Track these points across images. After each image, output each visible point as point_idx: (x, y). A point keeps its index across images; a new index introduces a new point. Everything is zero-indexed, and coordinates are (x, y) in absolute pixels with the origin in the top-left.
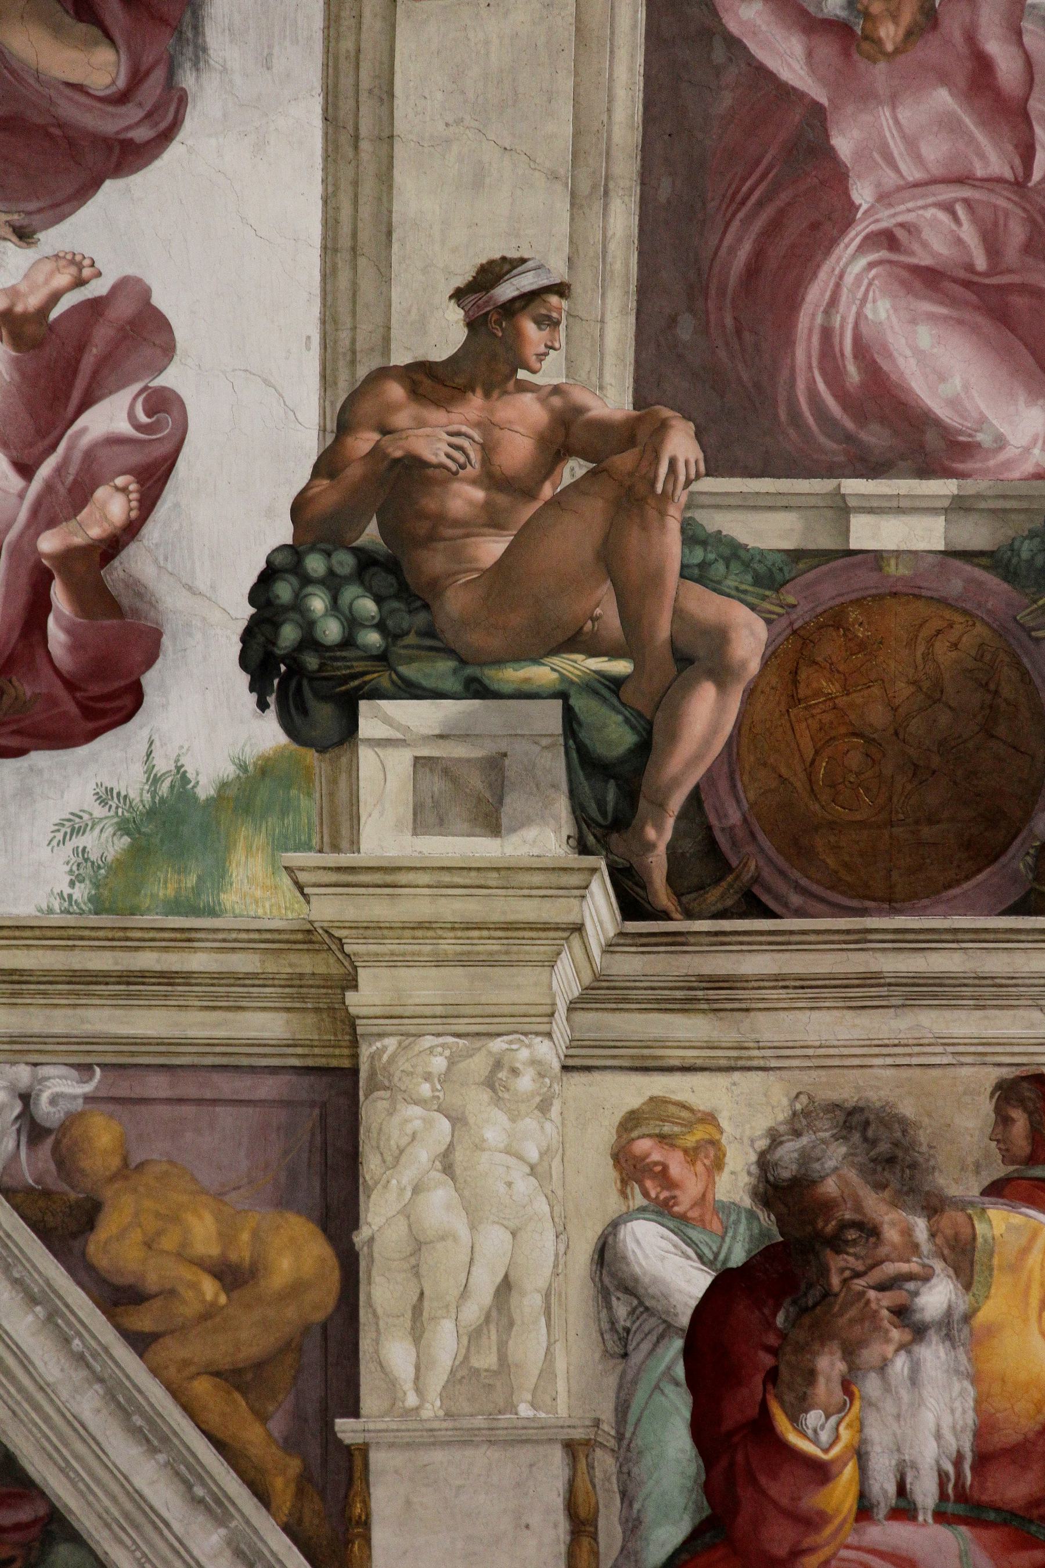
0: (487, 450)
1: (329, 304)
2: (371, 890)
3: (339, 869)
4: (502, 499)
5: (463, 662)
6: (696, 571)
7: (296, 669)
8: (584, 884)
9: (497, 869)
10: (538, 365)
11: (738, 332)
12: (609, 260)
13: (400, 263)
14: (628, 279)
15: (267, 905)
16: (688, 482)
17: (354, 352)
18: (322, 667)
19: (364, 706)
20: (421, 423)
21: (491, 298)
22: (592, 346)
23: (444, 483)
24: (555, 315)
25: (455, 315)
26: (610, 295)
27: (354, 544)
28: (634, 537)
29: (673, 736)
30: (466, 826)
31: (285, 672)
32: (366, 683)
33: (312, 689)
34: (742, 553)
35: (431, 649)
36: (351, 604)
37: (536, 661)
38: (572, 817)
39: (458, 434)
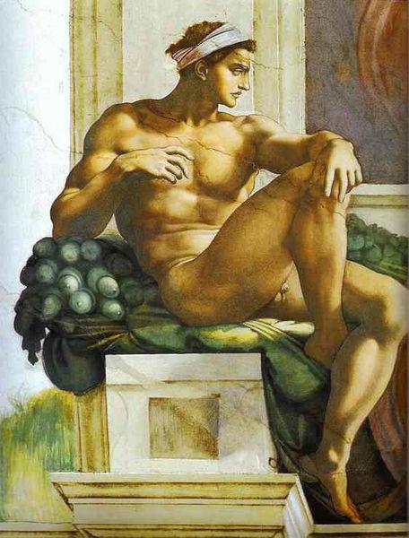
0: (197, 165)
1: (75, 58)
2: (120, 501)
3: (95, 484)
4: (209, 202)
5: (184, 325)
6: (359, 255)
7: (57, 332)
8: (283, 495)
9: (217, 484)
11: (383, 75)
12: (284, 23)
15: (40, 512)
16: (350, 188)
17: (95, 94)
18: (77, 330)
19: (110, 359)
23: (165, 189)
24: (244, 64)
28: (310, 231)
29: (346, 382)
30: (191, 450)
32: (111, 342)
33: (70, 346)
34: (394, 242)
35: (160, 315)
36: (98, 281)
37: (239, 324)
38: (271, 443)
39: (175, 153)
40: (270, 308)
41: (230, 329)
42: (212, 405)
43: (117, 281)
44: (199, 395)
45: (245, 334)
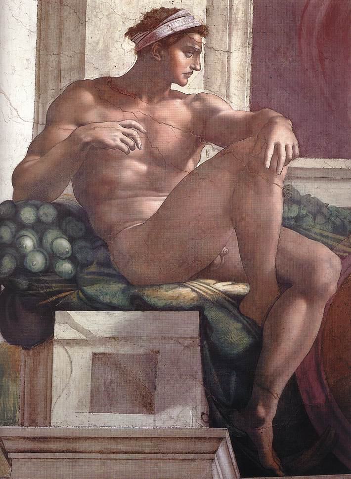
0: (150, 137)
1: (42, 38)
2: (58, 455)
3: (34, 439)
4: (158, 171)
6: (293, 222)
8: (213, 449)
9: (151, 438)
10: (186, 80)
12: (234, 11)
13: (92, 11)
14: (247, 23)
16: (288, 161)
17: (59, 70)
18: (30, 287)
20: (104, 119)
21: (155, 34)
22: (223, 68)
23: (119, 159)
24: (197, 47)
25: (129, 46)
26: (234, 33)
27: (55, 201)
29: (276, 338)
31: (4, 290)
34: (325, 211)
35: (108, 275)
36: (52, 242)
37: (181, 284)
40: (208, 271)
41: (172, 289)
42: (151, 359)
43: (69, 241)
44: (141, 351)
45: (186, 293)
